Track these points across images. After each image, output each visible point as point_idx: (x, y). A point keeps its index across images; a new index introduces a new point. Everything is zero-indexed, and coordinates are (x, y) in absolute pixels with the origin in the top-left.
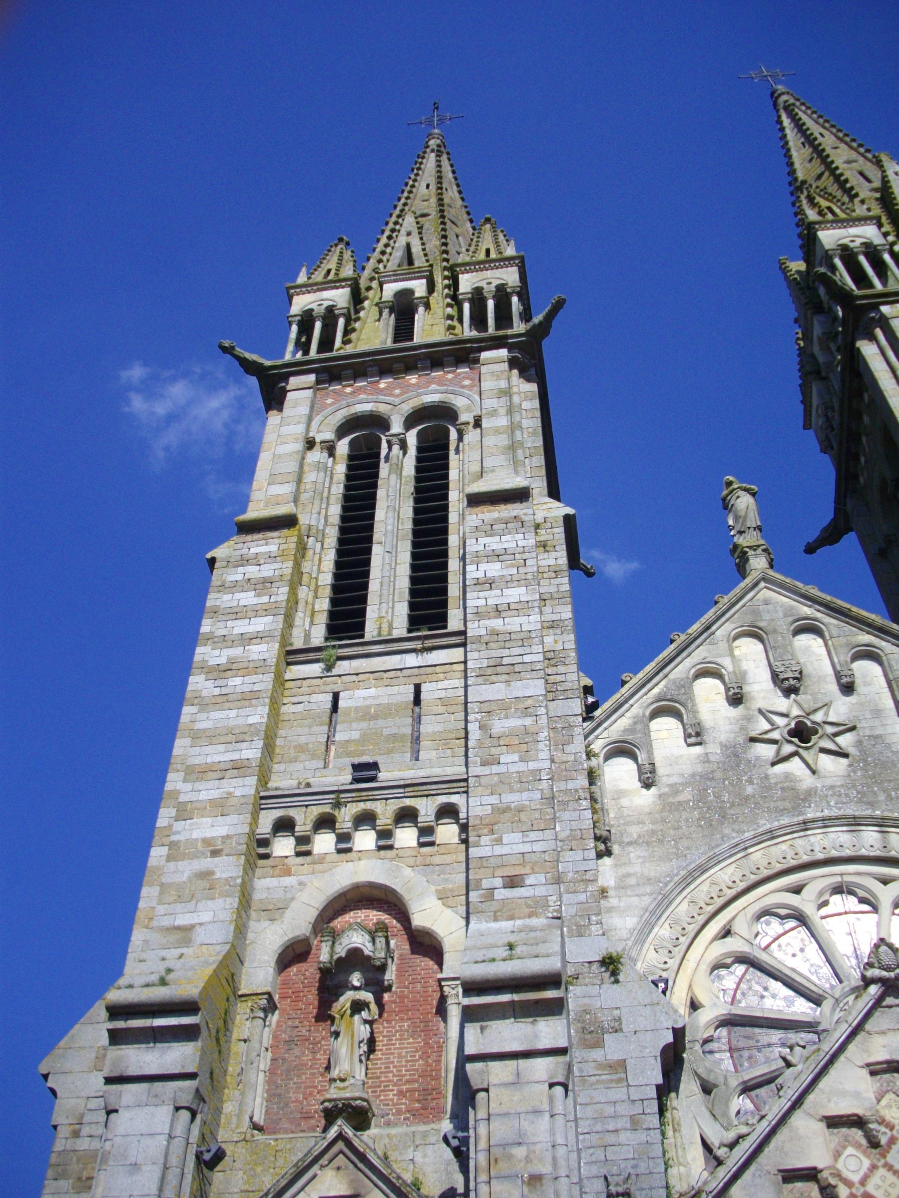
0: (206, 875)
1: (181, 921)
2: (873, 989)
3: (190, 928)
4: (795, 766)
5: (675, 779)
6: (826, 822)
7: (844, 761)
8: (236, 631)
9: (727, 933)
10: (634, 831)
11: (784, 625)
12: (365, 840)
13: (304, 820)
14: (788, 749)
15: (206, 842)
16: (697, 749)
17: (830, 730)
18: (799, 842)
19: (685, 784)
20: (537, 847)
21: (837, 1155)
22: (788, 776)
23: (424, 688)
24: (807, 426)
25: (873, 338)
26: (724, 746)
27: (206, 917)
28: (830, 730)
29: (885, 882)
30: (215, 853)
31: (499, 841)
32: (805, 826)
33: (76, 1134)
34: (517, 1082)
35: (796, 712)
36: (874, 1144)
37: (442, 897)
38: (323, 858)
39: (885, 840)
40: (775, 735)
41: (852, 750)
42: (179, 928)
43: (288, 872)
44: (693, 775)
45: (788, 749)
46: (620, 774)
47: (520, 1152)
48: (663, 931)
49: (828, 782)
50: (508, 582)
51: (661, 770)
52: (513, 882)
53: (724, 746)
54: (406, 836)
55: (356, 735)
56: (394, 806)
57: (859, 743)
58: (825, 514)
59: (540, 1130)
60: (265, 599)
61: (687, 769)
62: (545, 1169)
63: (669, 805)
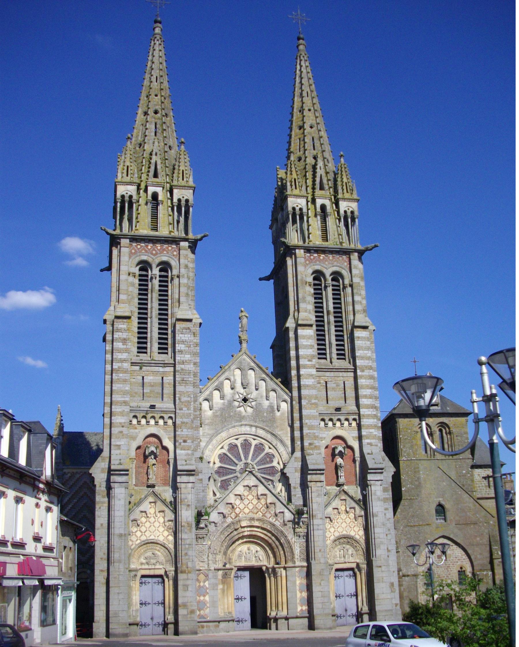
0: (121, 432)
1: (118, 443)
2: (247, 472)
3: (120, 446)
4: (242, 409)
5: (217, 409)
6: (246, 425)
7: (252, 409)
8: (119, 357)
9: (222, 448)
10: (207, 421)
11: (247, 368)
12: (152, 422)
13: (139, 416)
14: (241, 404)
15: (120, 423)
16: (222, 401)
17: (251, 400)
18: (240, 429)
19: (219, 410)
20: (190, 433)
21: (236, 500)
22: (240, 411)
23: (164, 378)
24: (271, 227)
25: (291, 257)
26: (228, 401)
27: (123, 443)
28: (251, 400)
29: (254, 439)
30: (123, 427)
31: (182, 431)
32: (241, 425)
33: (100, 486)
34: (186, 488)
35: (245, 394)
36: (242, 499)
37: (169, 438)
38: (143, 426)
39: (256, 431)
40: (239, 400)
41: (255, 407)
42: (117, 445)
43: (136, 428)
44: (221, 408)
45: (241, 404)
46: (205, 405)
47: (186, 500)
48: (210, 447)
49: (248, 414)
50: (186, 353)
51: (214, 406)
52: (185, 441)
53: (228, 401)
54: (161, 422)
55: (149, 391)
56: (159, 415)
57: (256, 405)
58: (268, 273)
59: (190, 497)
60: (125, 347)
61: (220, 406)
62: (190, 504)
63: (215, 416)
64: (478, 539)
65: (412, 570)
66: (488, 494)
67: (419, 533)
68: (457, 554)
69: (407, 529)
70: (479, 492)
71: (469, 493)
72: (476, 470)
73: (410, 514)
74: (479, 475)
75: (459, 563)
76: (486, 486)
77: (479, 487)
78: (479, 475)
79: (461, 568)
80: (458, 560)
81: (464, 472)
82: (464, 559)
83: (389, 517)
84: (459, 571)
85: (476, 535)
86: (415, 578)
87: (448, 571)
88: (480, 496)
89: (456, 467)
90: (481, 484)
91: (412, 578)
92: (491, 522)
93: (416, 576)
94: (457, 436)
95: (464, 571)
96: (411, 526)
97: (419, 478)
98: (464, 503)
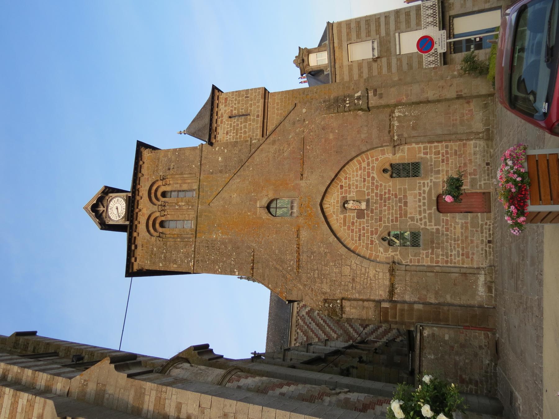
64: (331, 136)
65: (381, 274)
66: (258, 116)
67: (312, 253)
68: (358, 178)
69: (304, 276)
70: (253, 133)
71: (253, 150)
72: (219, 137)
73: (278, 266)
74: (227, 133)
75: (375, 176)
76: (246, 121)
77: (245, 132)
78: (227, 133)
79: (385, 171)
80: (369, 177)
81: (220, 159)
82: (368, 164)
83: (196, 405)
84: (391, 176)
85: (323, 140)
86: (397, 273)
87: (389, 198)
88: (259, 132)
89: (212, 173)
90: (241, 128)
91: (397, 279)
92: (304, 110)
93: (393, 268)
94: (169, 169)
95: (391, 165)
96: (299, 267)
97: (223, 243)
98: (268, 162)
